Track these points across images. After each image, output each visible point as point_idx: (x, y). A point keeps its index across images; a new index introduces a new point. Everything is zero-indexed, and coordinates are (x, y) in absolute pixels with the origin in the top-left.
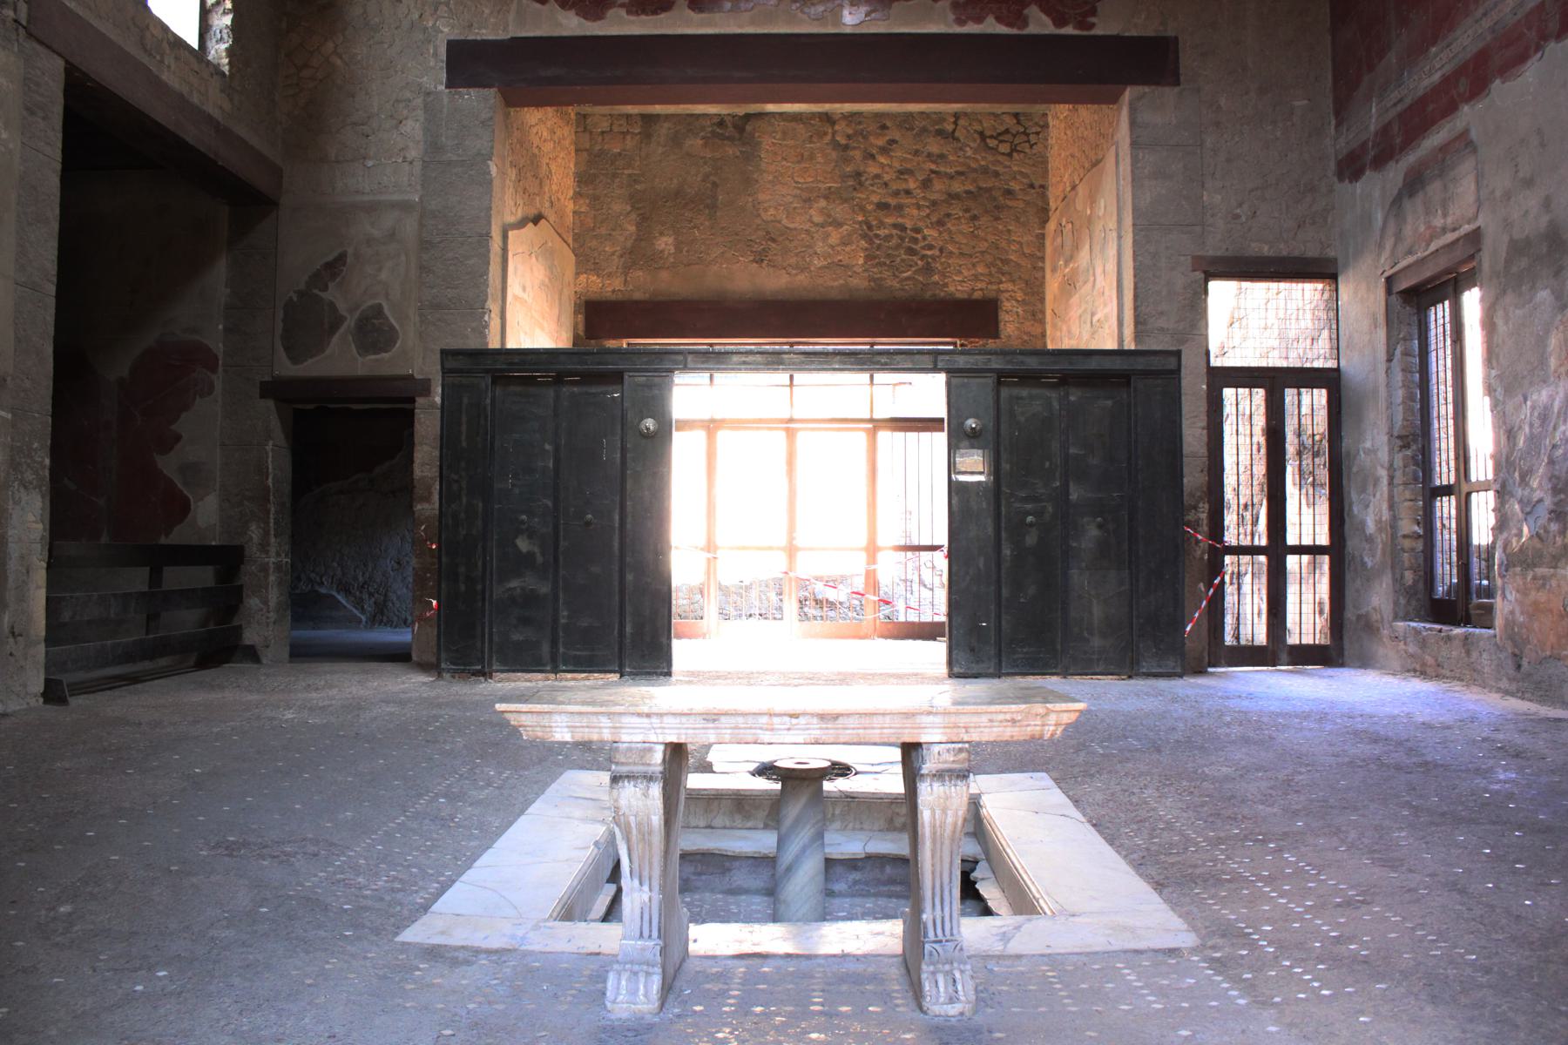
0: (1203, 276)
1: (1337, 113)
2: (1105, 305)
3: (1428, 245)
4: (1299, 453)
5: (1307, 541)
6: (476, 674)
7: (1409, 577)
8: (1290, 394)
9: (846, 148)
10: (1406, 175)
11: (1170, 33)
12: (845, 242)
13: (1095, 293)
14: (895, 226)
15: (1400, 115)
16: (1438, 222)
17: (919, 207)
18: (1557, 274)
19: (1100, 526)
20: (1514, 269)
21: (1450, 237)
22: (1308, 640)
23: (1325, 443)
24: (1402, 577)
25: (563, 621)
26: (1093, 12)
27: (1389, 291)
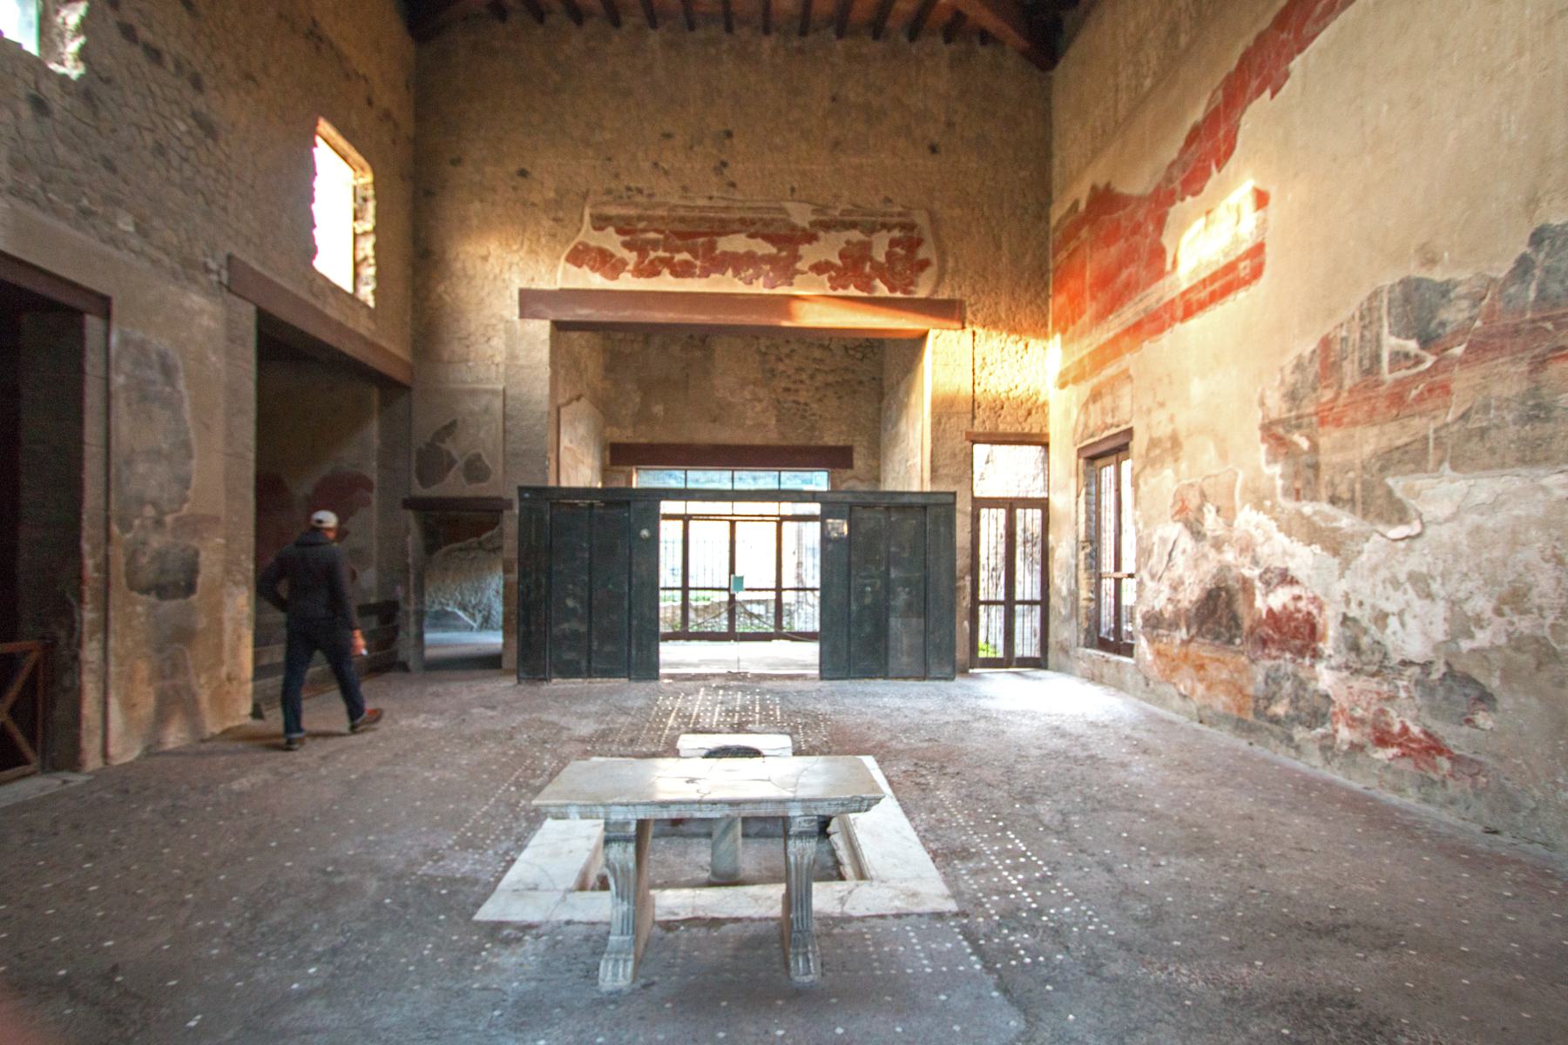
0: (968, 444)
4: (1025, 543)
5: (1028, 598)
7: (1085, 625)
8: (1019, 512)
9: (766, 354)
12: (764, 411)
15: (1090, 354)
16: (1109, 420)
17: (808, 391)
18: (1176, 460)
19: (909, 593)
20: (1152, 454)
21: (1114, 431)
22: (1027, 654)
23: (1039, 539)
26: (912, 283)
27: (1079, 457)
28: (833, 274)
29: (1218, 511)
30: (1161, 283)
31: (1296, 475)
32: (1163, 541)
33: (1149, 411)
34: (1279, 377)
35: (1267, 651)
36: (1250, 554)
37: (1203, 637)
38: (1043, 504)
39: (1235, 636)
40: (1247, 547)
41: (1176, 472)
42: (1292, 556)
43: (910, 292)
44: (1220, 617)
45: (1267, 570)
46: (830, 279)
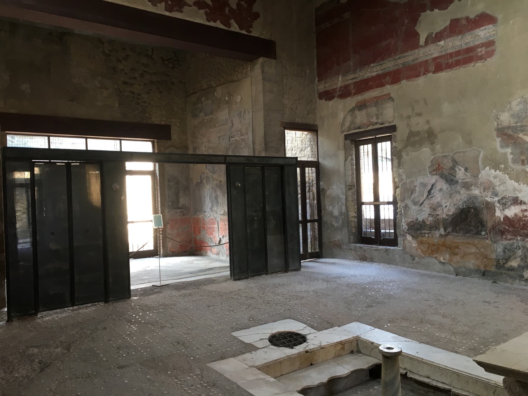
1: (319, 76)
2: (242, 135)
3: (368, 127)
6: (31, 315)
8: (307, 169)
10: (357, 103)
11: (273, 39)
13: (232, 129)
14: (131, 92)
15: (355, 83)
16: (374, 120)
18: (432, 143)
20: (412, 140)
24: (352, 230)
25: (76, 281)
27: (346, 139)
28: (207, 10)
29: (466, 170)
30: (416, 51)
31: (522, 153)
32: (424, 185)
33: (409, 117)
34: (508, 106)
35: (504, 236)
36: (491, 190)
37: (457, 232)
38: (315, 165)
39: (481, 231)
40: (489, 187)
41: (433, 150)
42: (520, 191)
43: (251, 32)
44: (470, 222)
45: (502, 198)
46: (206, 13)
